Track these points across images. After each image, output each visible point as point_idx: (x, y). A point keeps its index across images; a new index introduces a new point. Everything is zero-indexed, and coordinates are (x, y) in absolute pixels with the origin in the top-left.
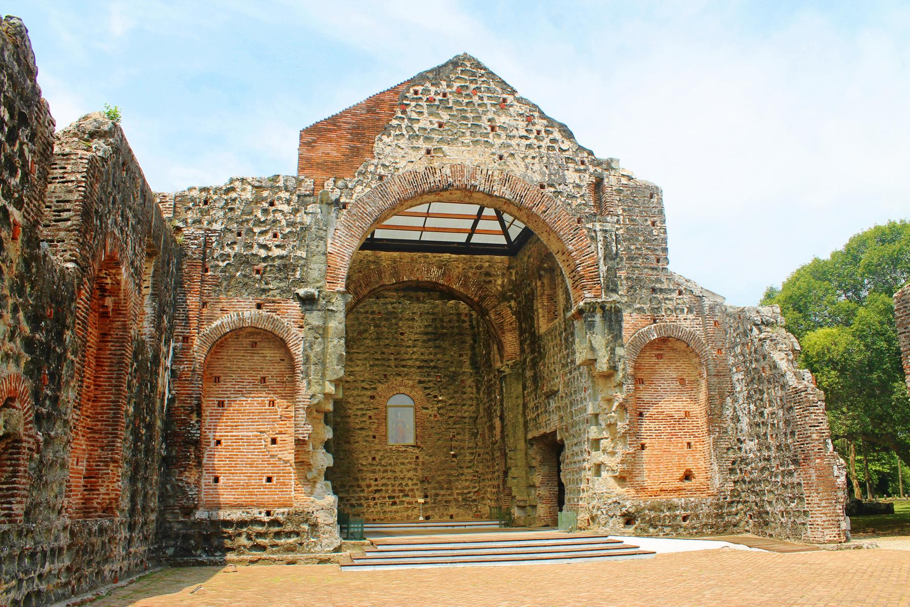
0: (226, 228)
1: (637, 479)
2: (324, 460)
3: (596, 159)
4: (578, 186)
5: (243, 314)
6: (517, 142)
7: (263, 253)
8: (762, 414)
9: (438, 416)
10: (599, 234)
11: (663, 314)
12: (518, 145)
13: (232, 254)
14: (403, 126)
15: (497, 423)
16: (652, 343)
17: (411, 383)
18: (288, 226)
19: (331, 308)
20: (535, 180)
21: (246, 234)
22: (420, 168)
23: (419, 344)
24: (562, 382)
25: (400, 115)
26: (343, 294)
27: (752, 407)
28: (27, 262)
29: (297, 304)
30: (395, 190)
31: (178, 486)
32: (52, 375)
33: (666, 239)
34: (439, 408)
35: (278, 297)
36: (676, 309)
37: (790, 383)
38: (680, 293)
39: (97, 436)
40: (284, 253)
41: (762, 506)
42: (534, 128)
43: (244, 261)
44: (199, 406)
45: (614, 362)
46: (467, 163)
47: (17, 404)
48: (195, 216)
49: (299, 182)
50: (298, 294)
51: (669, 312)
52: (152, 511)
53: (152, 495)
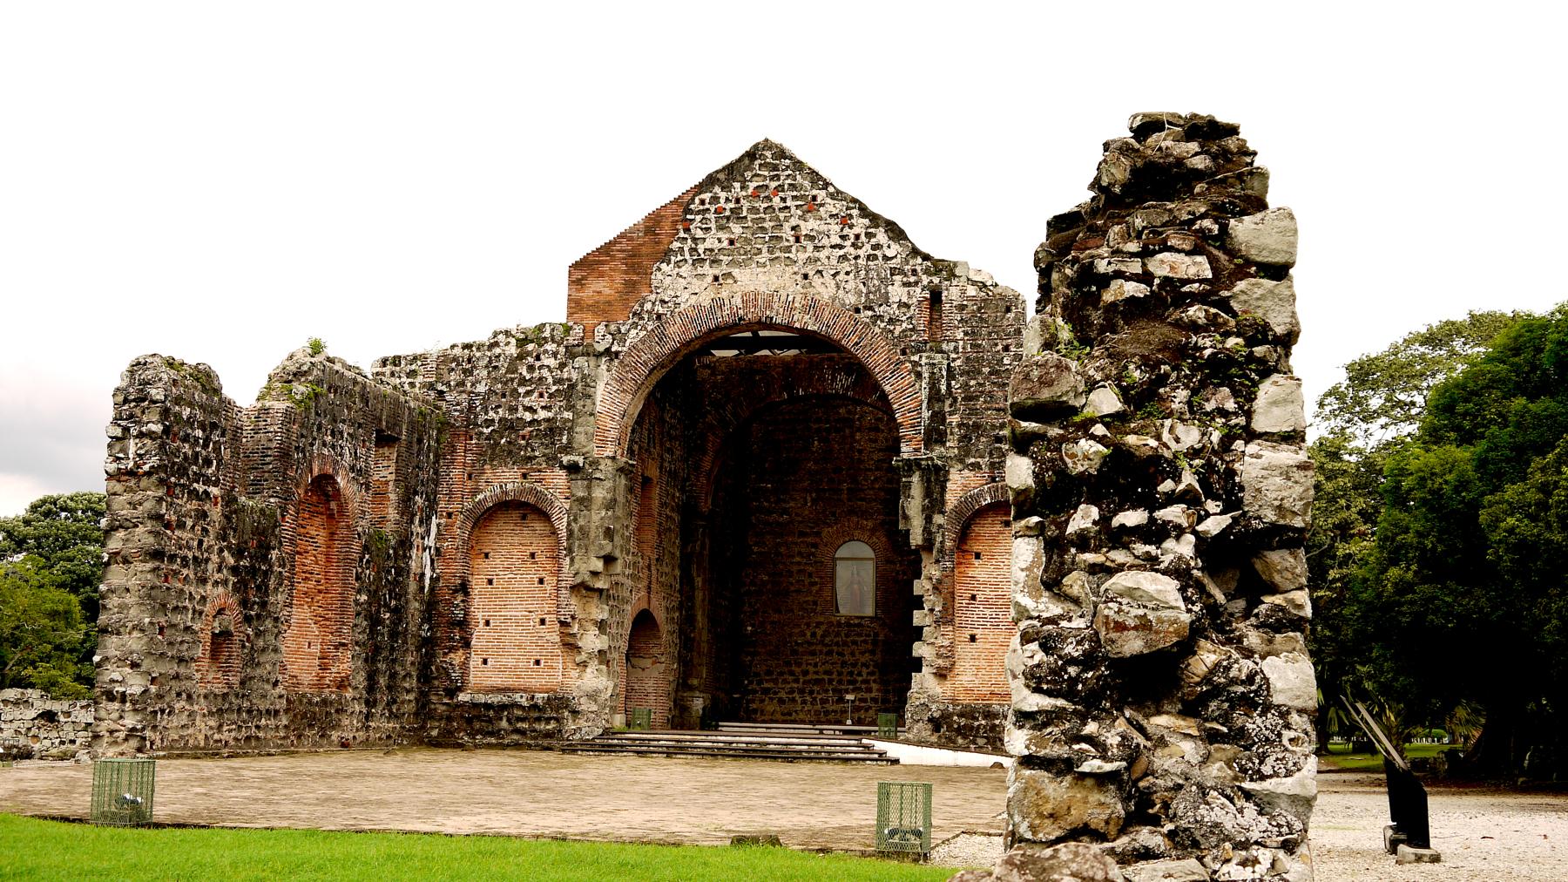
1: (960, 678)
3: (936, 262)
4: (907, 306)
7: (528, 416)
12: (829, 258)
13: (497, 419)
14: (686, 249)
17: (870, 524)
18: (554, 385)
19: (598, 475)
20: (847, 302)
21: (511, 396)
22: (705, 300)
25: (682, 234)
26: (613, 458)
28: (228, 518)
29: (563, 473)
30: (676, 333)
31: (443, 668)
32: (259, 588)
35: (544, 465)
39: (328, 623)
40: (550, 415)
42: (851, 233)
43: (509, 426)
45: (930, 533)
46: (762, 289)
47: (227, 612)
49: (568, 330)
52: (408, 691)
53: (405, 677)
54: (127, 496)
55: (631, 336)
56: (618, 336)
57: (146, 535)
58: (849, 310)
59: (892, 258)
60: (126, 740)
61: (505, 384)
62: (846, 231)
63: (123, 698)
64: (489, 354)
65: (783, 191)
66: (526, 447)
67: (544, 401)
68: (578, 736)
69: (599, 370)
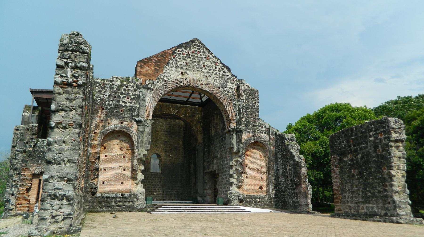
0: (110, 94)
1: (244, 188)
2: (141, 176)
3: (238, 80)
4: (231, 88)
5: (116, 125)
6: (212, 72)
7: (123, 104)
8: (286, 169)
9: (170, 162)
10: (237, 105)
11: (256, 134)
14: (174, 63)
15: (192, 166)
16: (252, 143)
18: (133, 95)
19: (146, 125)
20: (217, 85)
22: (179, 78)
23: (164, 135)
24: (220, 153)
26: (151, 120)
27: (283, 166)
29: (135, 123)
30: (170, 86)
31: (91, 184)
33: (259, 108)
34: (170, 160)
35: (128, 120)
36: (260, 132)
37: (296, 160)
38: (262, 127)
40: (131, 105)
41: (285, 199)
42: (218, 67)
44: (99, 157)
45: (239, 149)
46: (195, 78)
48: (99, 89)
50: (136, 120)
51: (258, 133)
54: (64, 95)
55: (157, 85)
56: (154, 85)
57: (77, 116)
58: (217, 87)
59: (228, 76)
60: (63, 220)
61: (116, 93)
62: (217, 66)
63: (63, 197)
64: (110, 83)
65: (201, 53)
66: (122, 114)
67: (129, 100)
68: (139, 207)
69: (147, 94)
